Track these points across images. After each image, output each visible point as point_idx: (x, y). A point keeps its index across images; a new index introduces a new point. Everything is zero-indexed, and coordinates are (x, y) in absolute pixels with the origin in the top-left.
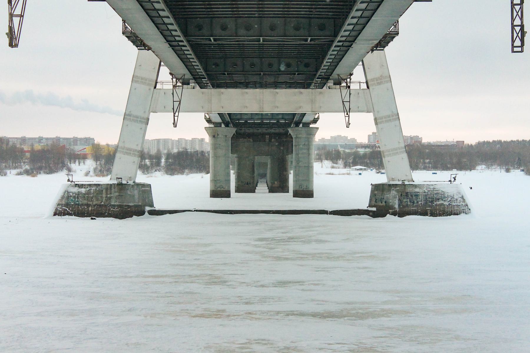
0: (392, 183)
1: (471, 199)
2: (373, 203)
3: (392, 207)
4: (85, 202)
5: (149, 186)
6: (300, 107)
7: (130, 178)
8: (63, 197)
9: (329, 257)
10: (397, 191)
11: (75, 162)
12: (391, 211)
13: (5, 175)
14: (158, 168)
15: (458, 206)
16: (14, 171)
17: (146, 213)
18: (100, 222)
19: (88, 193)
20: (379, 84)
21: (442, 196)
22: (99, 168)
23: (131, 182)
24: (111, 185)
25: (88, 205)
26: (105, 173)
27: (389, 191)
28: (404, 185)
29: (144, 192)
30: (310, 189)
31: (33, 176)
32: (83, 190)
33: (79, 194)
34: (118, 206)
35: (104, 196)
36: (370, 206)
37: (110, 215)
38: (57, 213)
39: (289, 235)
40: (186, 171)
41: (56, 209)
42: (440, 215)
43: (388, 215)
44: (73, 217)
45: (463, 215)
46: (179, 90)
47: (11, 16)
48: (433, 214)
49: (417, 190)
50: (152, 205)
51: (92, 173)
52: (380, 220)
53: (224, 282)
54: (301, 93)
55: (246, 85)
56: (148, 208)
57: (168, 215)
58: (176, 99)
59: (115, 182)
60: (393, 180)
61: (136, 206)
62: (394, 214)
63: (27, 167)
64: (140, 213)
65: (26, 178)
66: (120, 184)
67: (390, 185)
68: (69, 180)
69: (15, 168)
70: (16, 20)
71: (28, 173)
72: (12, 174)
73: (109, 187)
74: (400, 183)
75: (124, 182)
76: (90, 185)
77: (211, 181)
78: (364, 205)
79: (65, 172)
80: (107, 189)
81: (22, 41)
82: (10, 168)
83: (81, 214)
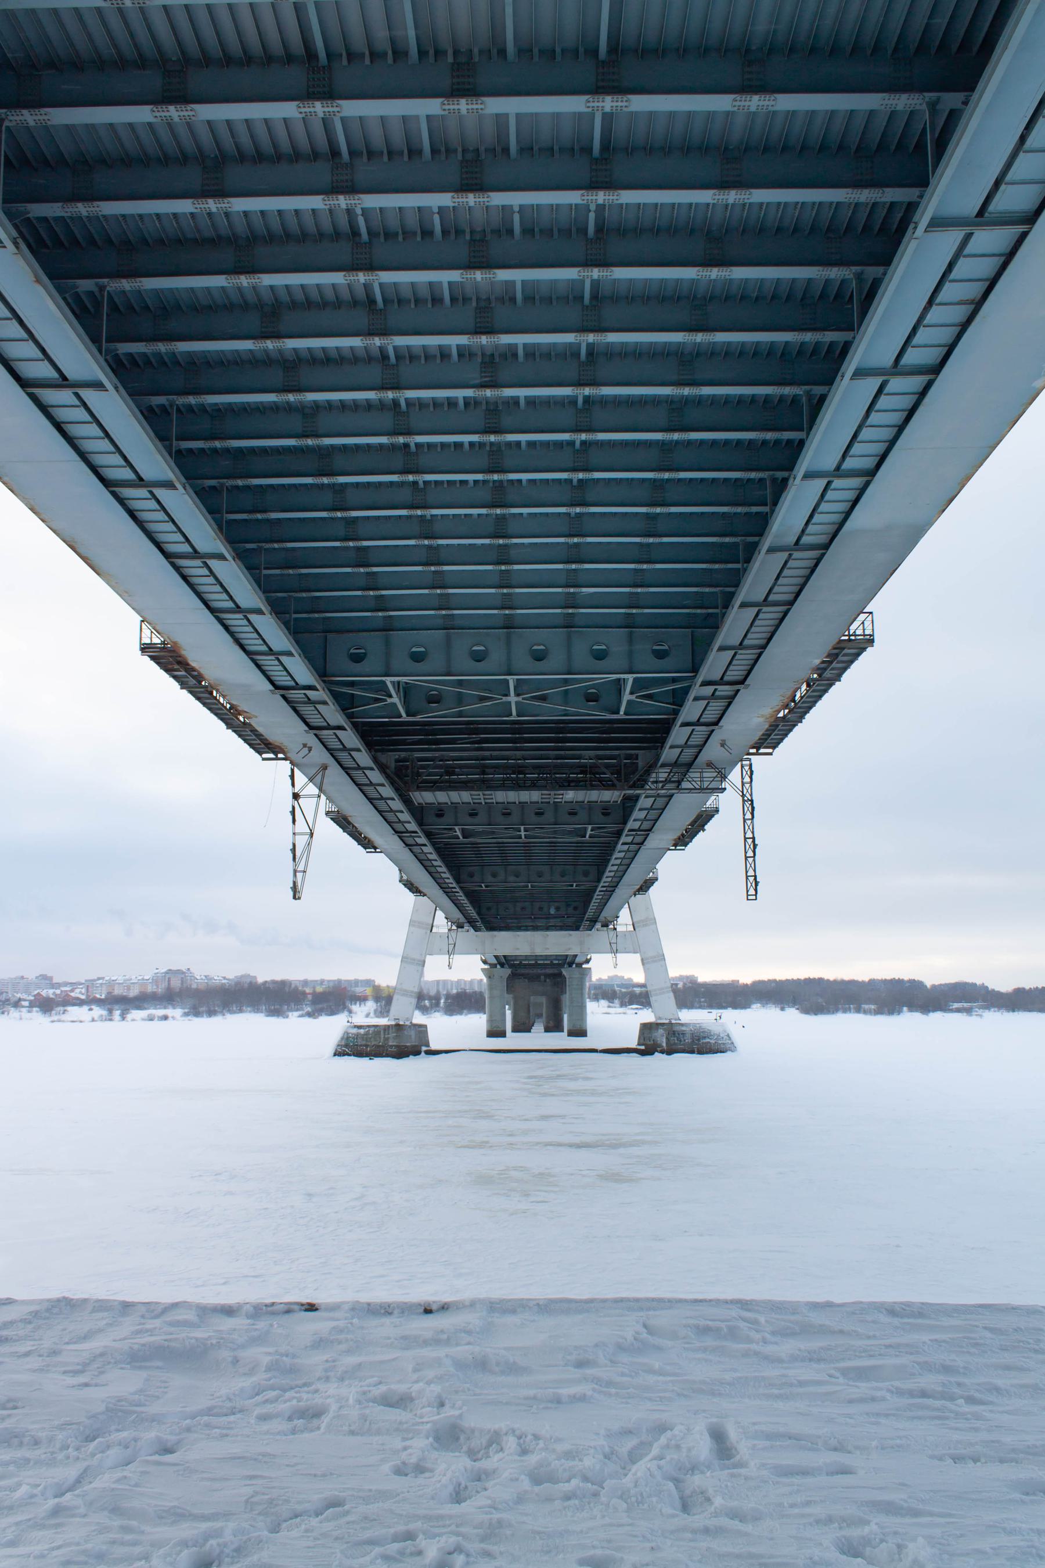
0: (659, 1021)
1: (738, 1037)
2: (642, 1041)
3: (660, 1046)
4: (364, 1043)
5: (425, 1026)
7: (407, 1019)
8: (342, 1038)
9: (593, 1093)
10: (664, 1029)
11: (355, 1004)
12: (659, 1049)
15: (724, 1044)
16: (296, 1014)
17: (423, 1053)
19: (367, 1034)
20: (646, 925)
21: (707, 1034)
22: (379, 1009)
23: (408, 1023)
24: (389, 1026)
25: (367, 1046)
27: (657, 1029)
28: (671, 1024)
29: (420, 1032)
32: (362, 1031)
33: (358, 1035)
34: (396, 1046)
35: (382, 1036)
36: (638, 1045)
37: (387, 1056)
38: (337, 1054)
39: (558, 1073)
41: (336, 1050)
42: (707, 1053)
43: (656, 1053)
44: (352, 1057)
45: (729, 1053)
46: (453, 934)
47: (295, 872)
48: (700, 1052)
49: (684, 1028)
50: (428, 1045)
51: (372, 1015)
52: (648, 1058)
53: (489, 1117)
55: (519, 928)
56: (424, 1048)
57: (444, 1055)
59: (393, 1023)
60: (660, 1018)
62: (662, 1052)
63: (309, 1009)
64: (417, 1053)
65: (307, 1020)
66: (398, 1025)
67: (658, 1024)
69: (297, 1010)
70: (299, 875)
71: (309, 1015)
72: (293, 1016)
73: (387, 1028)
74: (667, 1021)
75: (401, 1023)
76: (369, 1026)
78: (633, 1043)
79: (346, 1013)
80: (385, 1030)
81: (305, 894)
82: (292, 1011)
83: (359, 1054)
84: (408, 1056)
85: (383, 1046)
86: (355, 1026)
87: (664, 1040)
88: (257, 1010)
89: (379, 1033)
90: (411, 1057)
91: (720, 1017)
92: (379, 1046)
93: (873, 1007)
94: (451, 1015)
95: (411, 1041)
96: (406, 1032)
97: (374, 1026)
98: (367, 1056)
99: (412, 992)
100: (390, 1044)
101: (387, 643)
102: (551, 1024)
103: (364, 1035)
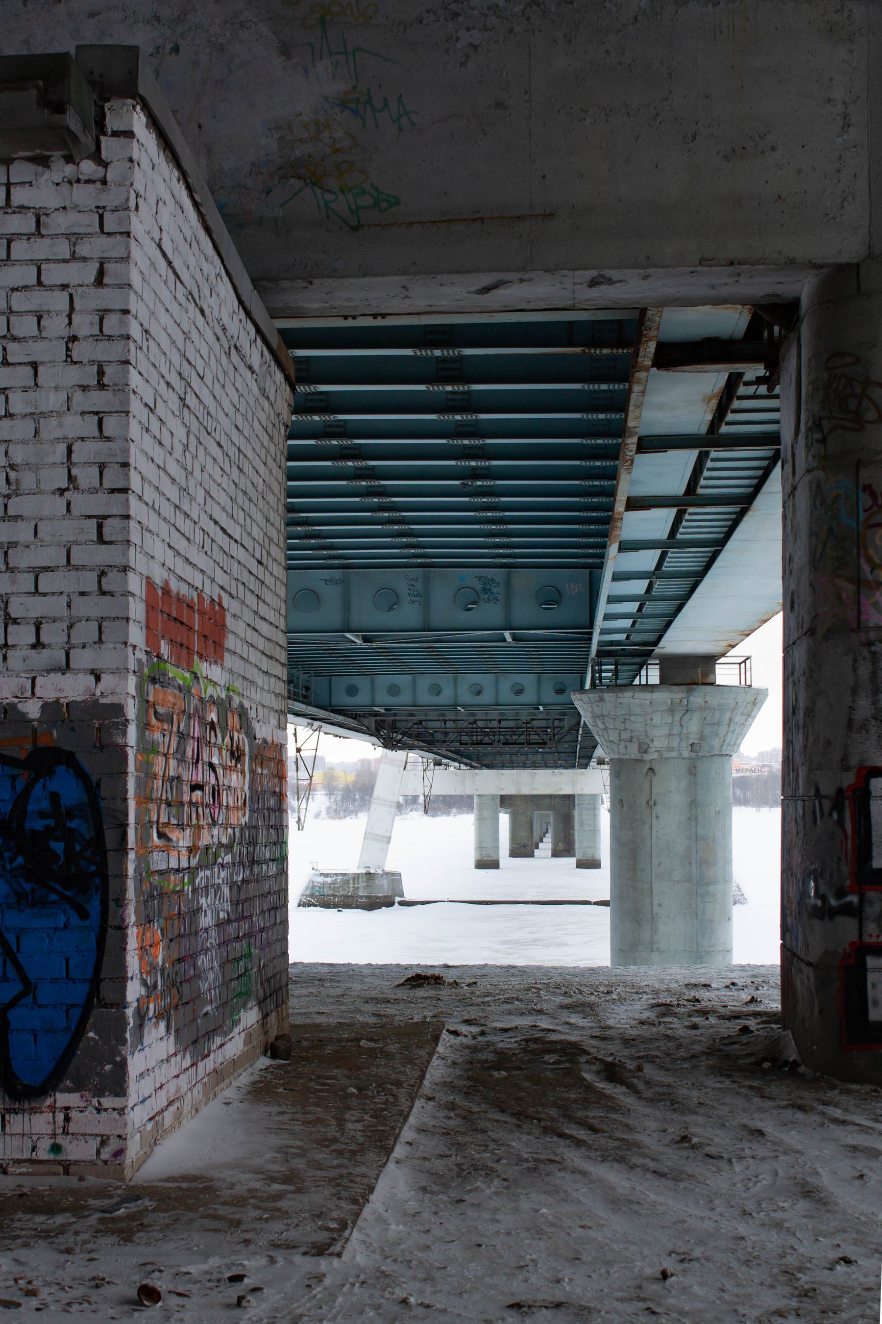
4: (331, 892)
6: (561, 789)
7: (379, 867)
8: (307, 888)
14: (415, 806)
17: (396, 904)
18: (346, 912)
19: (334, 883)
22: (334, 807)
23: (380, 871)
25: (334, 896)
26: (342, 814)
29: (394, 881)
30: (597, 858)
32: (329, 880)
33: (324, 884)
34: (365, 896)
35: (351, 886)
37: (357, 907)
38: (299, 905)
39: (535, 936)
40: (454, 810)
41: (301, 900)
44: (319, 908)
50: (402, 896)
51: (324, 814)
54: (561, 774)
55: (503, 767)
56: (397, 899)
57: (419, 906)
58: (427, 783)
59: (364, 871)
61: (385, 897)
64: (390, 904)
68: (313, 869)
73: (357, 877)
75: (372, 871)
77: (476, 848)
80: (354, 879)
83: (327, 905)
85: (352, 896)
89: (347, 882)
92: (347, 896)
95: (382, 889)
96: (377, 882)
97: (342, 874)
98: (335, 906)
101: (372, 683)
102: (561, 846)
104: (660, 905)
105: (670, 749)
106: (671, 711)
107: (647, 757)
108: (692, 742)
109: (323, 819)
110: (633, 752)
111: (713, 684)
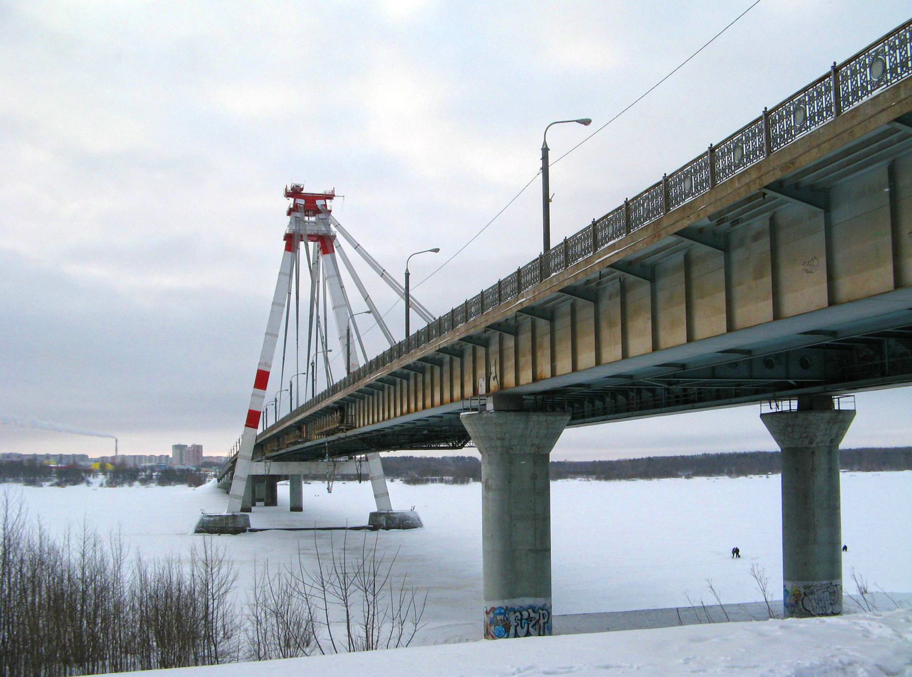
2: (371, 523)
3: (383, 526)
4: (213, 525)
8: (200, 523)
11: (89, 476)
13: (41, 486)
14: (152, 481)
15: (416, 523)
16: (48, 483)
17: (247, 531)
19: (215, 520)
22: (109, 481)
25: (215, 527)
26: (114, 484)
27: (381, 516)
31: (63, 487)
32: (212, 519)
33: (210, 520)
35: (224, 522)
36: (369, 524)
38: (198, 531)
40: (173, 483)
45: (419, 528)
48: (404, 528)
49: (395, 515)
50: (250, 527)
51: (104, 484)
52: (375, 533)
56: (248, 528)
58: (267, 469)
59: (231, 514)
60: (382, 510)
61: (242, 527)
62: (383, 529)
64: (244, 531)
65: (57, 488)
68: (202, 513)
71: (59, 484)
74: (386, 512)
75: (235, 514)
82: (44, 481)
84: (240, 533)
86: (208, 516)
87: (385, 522)
88: (17, 481)
90: (242, 533)
91: (414, 508)
92: (222, 527)
93: (451, 478)
94: (163, 485)
95: (241, 523)
99: (240, 496)
100: (230, 526)
102: (269, 500)
103: (213, 521)
104: (818, 521)
105: (822, 442)
106: (829, 423)
107: (812, 446)
108: (832, 438)
109: (105, 487)
110: (806, 443)
111: (831, 409)
